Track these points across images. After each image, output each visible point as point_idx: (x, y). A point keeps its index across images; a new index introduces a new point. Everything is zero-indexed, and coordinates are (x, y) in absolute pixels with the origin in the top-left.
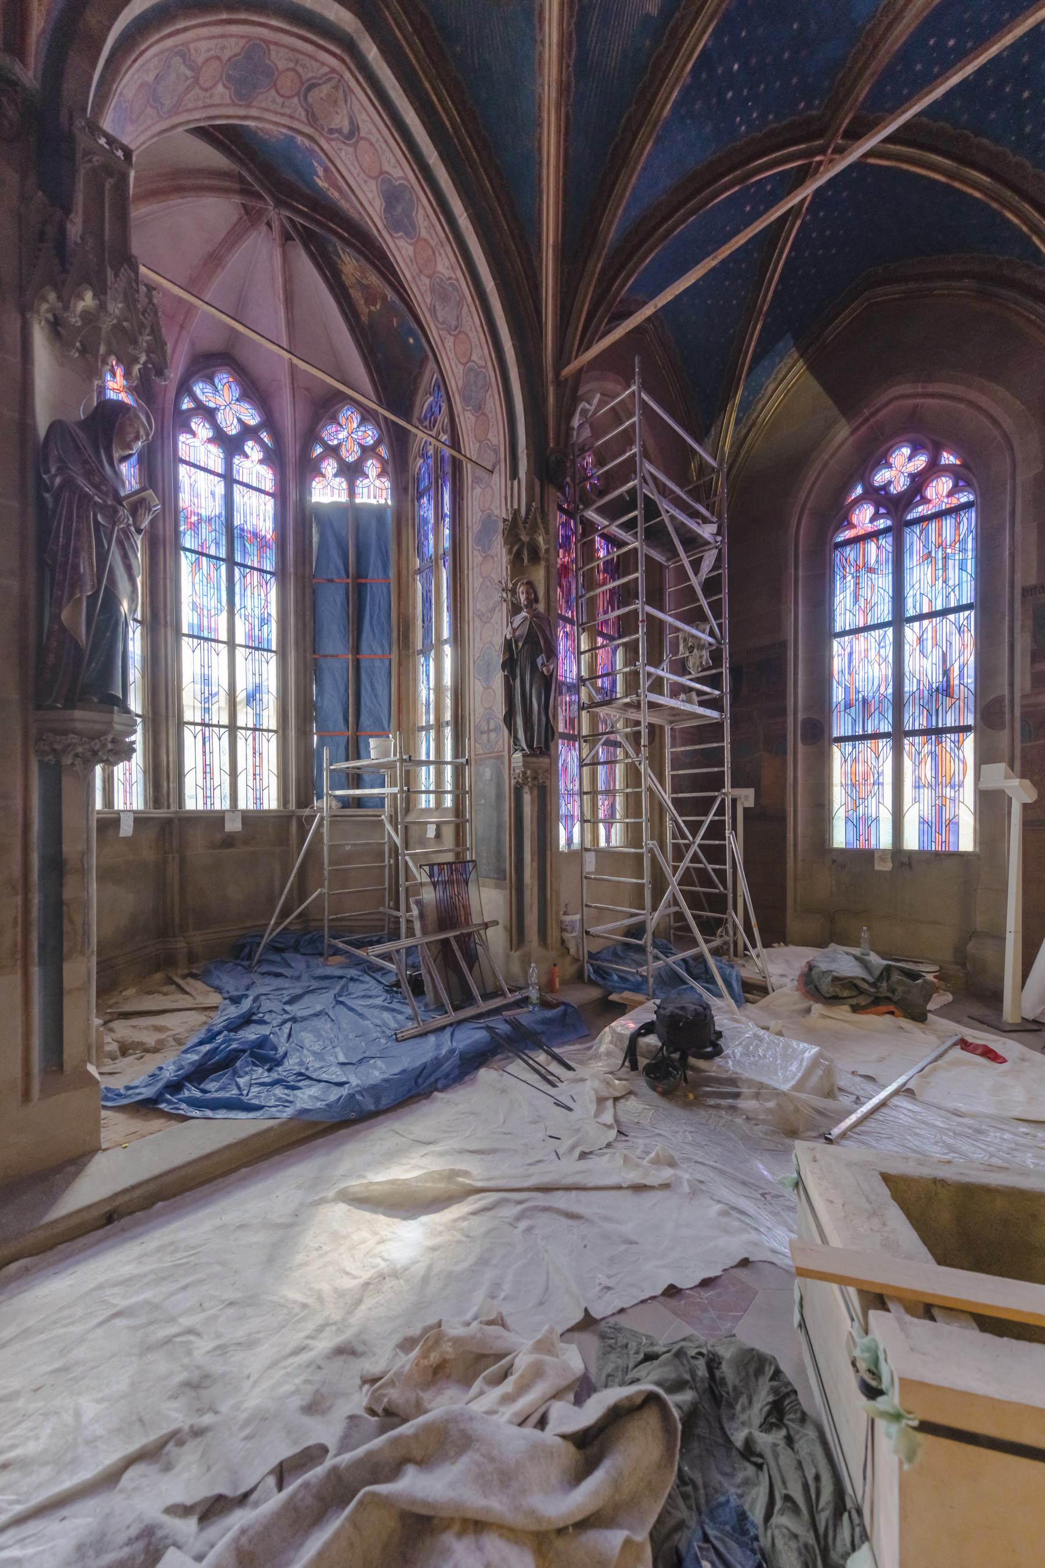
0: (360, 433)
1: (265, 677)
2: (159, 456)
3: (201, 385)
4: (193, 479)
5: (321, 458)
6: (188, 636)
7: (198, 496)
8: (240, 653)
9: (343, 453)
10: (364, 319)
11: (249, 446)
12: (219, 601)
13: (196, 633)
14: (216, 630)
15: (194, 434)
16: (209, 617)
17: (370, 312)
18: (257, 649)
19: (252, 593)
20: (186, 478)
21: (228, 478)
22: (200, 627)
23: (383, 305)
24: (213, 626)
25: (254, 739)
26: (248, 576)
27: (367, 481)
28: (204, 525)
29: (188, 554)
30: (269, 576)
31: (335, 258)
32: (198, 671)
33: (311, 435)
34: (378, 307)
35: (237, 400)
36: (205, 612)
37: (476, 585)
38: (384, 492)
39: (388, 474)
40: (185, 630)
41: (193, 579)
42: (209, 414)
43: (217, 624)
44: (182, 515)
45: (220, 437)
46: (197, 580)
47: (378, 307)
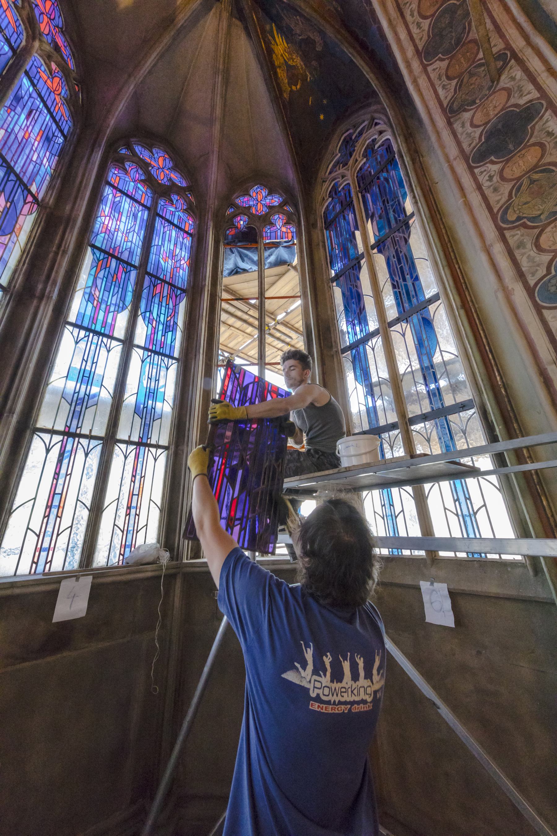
0: (268, 201)
2: (85, 161)
3: (140, 148)
4: (118, 199)
5: (235, 216)
6: (75, 325)
7: (120, 213)
8: (136, 356)
9: (253, 211)
10: (285, 95)
11: (175, 197)
12: (123, 299)
13: (85, 324)
14: (113, 327)
15: (126, 171)
16: (107, 312)
17: (291, 91)
18: (156, 353)
19: (160, 302)
20: (110, 196)
22: (94, 319)
23: (302, 84)
24: (109, 320)
26: (159, 286)
27: (275, 228)
28: (120, 234)
29: (95, 250)
30: (179, 292)
31: (270, 38)
32: (77, 364)
33: (227, 200)
34: (298, 87)
35: (169, 169)
36: (103, 306)
37: (493, 198)
38: (290, 235)
39: (294, 221)
40: (72, 318)
42: (144, 166)
43: (114, 319)
44: (99, 219)
45: (149, 181)
46: (101, 274)
47: (298, 87)
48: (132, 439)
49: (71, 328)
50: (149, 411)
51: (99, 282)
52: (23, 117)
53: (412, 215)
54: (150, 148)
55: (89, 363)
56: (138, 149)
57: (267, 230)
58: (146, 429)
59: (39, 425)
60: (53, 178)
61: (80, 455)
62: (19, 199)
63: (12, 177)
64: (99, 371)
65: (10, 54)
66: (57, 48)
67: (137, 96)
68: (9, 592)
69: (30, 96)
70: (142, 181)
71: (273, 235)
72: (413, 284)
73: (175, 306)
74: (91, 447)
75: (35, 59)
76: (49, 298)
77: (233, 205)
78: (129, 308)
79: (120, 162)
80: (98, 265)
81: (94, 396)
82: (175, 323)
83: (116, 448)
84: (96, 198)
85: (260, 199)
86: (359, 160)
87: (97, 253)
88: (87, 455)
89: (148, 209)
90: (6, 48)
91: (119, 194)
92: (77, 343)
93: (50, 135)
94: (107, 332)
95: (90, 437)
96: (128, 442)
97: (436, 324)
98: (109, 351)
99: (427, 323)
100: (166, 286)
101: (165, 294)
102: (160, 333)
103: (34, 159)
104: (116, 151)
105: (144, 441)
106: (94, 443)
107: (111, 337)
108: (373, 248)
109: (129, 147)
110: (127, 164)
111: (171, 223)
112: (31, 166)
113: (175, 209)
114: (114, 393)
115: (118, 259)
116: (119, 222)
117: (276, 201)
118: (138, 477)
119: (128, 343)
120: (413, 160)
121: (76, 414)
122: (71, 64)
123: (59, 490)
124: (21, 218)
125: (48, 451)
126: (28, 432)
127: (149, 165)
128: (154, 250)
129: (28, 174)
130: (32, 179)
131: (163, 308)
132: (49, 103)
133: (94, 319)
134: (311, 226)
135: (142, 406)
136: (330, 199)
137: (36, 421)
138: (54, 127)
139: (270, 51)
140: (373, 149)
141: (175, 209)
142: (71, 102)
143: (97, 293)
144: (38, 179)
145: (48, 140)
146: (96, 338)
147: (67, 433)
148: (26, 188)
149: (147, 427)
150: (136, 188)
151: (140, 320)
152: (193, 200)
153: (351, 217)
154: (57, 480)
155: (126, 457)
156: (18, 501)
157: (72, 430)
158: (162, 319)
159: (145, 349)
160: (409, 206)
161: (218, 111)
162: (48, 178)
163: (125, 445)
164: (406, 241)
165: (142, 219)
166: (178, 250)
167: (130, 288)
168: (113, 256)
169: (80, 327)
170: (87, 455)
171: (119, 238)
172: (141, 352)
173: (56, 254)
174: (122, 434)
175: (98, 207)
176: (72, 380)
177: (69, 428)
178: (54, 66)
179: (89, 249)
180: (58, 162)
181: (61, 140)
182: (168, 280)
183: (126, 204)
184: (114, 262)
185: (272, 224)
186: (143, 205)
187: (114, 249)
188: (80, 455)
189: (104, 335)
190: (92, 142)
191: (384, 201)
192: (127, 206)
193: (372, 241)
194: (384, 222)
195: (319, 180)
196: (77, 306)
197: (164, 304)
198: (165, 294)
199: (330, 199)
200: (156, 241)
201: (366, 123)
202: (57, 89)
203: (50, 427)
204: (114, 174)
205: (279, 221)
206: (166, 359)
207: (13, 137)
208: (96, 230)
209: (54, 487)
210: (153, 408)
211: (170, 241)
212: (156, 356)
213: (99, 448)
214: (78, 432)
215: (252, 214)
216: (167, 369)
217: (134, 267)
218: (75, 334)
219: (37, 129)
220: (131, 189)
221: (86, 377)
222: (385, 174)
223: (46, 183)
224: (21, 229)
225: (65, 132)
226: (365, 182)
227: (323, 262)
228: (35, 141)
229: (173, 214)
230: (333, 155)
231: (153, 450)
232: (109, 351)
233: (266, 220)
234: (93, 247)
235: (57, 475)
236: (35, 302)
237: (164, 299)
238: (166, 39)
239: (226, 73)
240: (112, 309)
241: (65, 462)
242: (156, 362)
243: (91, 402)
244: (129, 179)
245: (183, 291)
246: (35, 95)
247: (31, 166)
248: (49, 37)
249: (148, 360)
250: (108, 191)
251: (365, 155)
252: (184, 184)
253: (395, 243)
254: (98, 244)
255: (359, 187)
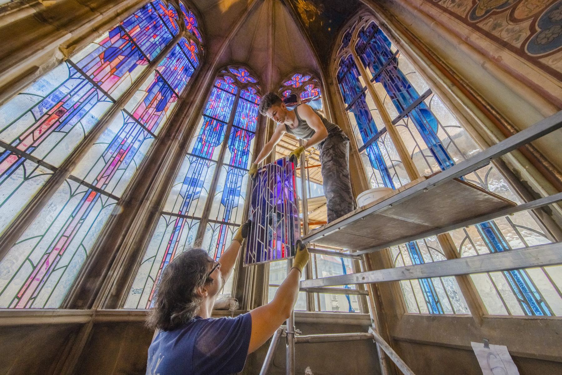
1: (239, 185)
6: (191, 155)
7: (220, 99)
10: (307, 25)
11: (250, 88)
12: (219, 140)
13: (197, 154)
15: (224, 80)
16: (209, 147)
17: (310, 22)
21: (238, 97)
22: (201, 151)
24: (210, 151)
25: (221, 231)
30: (251, 134)
36: (207, 144)
40: (190, 151)
41: (205, 128)
43: (213, 150)
45: (236, 82)
46: (208, 128)
48: (218, 220)
49: (189, 156)
50: (230, 202)
51: (206, 132)
52: (175, 61)
53: (398, 51)
54: (237, 68)
55: (197, 175)
56: (231, 70)
57: (303, 94)
58: (228, 213)
59: (164, 210)
60: (187, 86)
61: (186, 227)
62: (168, 95)
63: (166, 86)
64: (202, 179)
65: (172, 38)
66: (194, 34)
67: (230, 46)
68: (126, 318)
69: (179, 53)
70: (233, 83)
71: (307, 95)
72: (407, 91)
73: (248, 141)
74: (193, 224)
75: (183, 38)
76: (177, 138)
77: (282, 86)
78: (222, 144)
79: (222, 76)
80: (207, 124)
81: (198, 193)
82: (248, 151)
83: (208, 225)
84: (208, 92)
85: (297, 80)
86: (355, 40)
87: (207, 118)
88: (190, 229)
89: (235, 95)
90: (170, 36)
91: (220, 91)
92: (191, 164)
93: (188, 68)
94: (208, 158)
95: (193, 218)
96: (216, 222)
97: (434, 110)
98: (208, 168)
99: (426, 112)
100: (244, 131)
101: (243, 135)
102: (239, 156)
103: (178, 78)
104: (220, 72)
105: (226, 221)
106: (195, 221)
107: (211, 160)
108: (372, 81)
109: (226, 69)
110: (225, 78)
111: (249, 101)
112: (177, 81)
113: (250, 94)
114: (210, 191)
115: (217, 120)
116: (220, 105)
117: (307, 79)
118: (221, 245)
119: (220, 163)
120: (391, 21)
121: (186, 204)
122: (200, 40)
123: (170, 252)
124: (169, 104)
125: (167, 226)
126: (157, 214)
127: (235, 76)
128: (237, 114)
129: (174, 85)
130: (176, 86)
131: (241, 143)
132: (188, 55)
133: (201, 151)
134: (329, 85)
135: (226, 199)
136: (340, 67)
137: (163, 207)
138: (190, 65)
139: (296, 8)
140: (363, 32)
141: (250, 94)
142: (199, 55)
143: (205, 138)
144: (179, 86)
145: (186, 70)
146: (202, 161)
147: (180, 216)
148: (173, 91)
149: (228, 212)
150: (229, 87)
151: (228, 149)
152: (260, 88)
153: (354, 71)
154: (170, 244)
155: (214, 231)
156: (146, 258)
157: (183, 214)
158: (240, 149)
159: (230, 165)
160: (394, 48)
161: (271, 43)
162: (184, 86)
163: (214, 224)
164: (396, 68)
165: (232, 100)
166: (251, 113)
167: (223, 134)
168: (215, 119)
169: (194, 155)
170: (190, 229)
171: (219, 110)
172: (227, 167)
173: (184, 118)
174: (212, 217)
175: (209, 97)
176: (186, 184)
177: (181, 212)
178: (191, 41)
179: (203, 117)
180: (190, 79)
181: (193, 70)
182: (245, 128)
183: (224, 95)
184: (215, 122)
185: (305, 90)
186: (233, 94)
187: (216, 116)
188: (186, 227)
189: (206, 159)
190: (207, 69)
191: (375, 54)
192: (224, 95)
193: (371, 77)
194: (376, 65)
195: (332, 60)
196: (193, 144)
197: (242, 141)
198: (243, 135)
199: (340, 67)
200: (239, 109)
201: (357, 22)
202: (193, 51)
203: (170, 211)
204: (218, 83)
205: (309, 89)
206: (242, 171)
207: (169, 69)
208: (207, 108)
209: (168, 249)
210: (233, 200)
211: (246, 109)
212: (236, 170)
213: (198, 225)
214: (186, 214)
215: (293, 88)
216: (243, 176)
217: (226, 123)
218: (191, 159)
219: (181, 66)
220: (226, 88)
221: (193, 182)
222: (373, 40)
223: (183, 88)
224: (168, 108)
225: (195, 67)
226: (360, 50)
227: (339, 101)
228: (180, 70)
229: (249, 96)
230: (339, 45)
231: (231, 227)
232: (208, 168)
233: (302, 89)
234: (205, 115)
235: (171, 241)
236: (170, 142)
237: (242, 138)
238: (244, 17)
239: (274, 25)
240: (212, 145)
241: (177, 233)
242: (236, 173)
243: (196, 196)
244: (227, 84)
245: (253, 133)
246: (181, 53)
247: (177, 81)
248: (191, 31)
249: (231, 172)
250: (215, 90)
251: (359, 36)
252: (255, 81)
253: (387, 72)
254: (207, 114)
255: (358, 53)
